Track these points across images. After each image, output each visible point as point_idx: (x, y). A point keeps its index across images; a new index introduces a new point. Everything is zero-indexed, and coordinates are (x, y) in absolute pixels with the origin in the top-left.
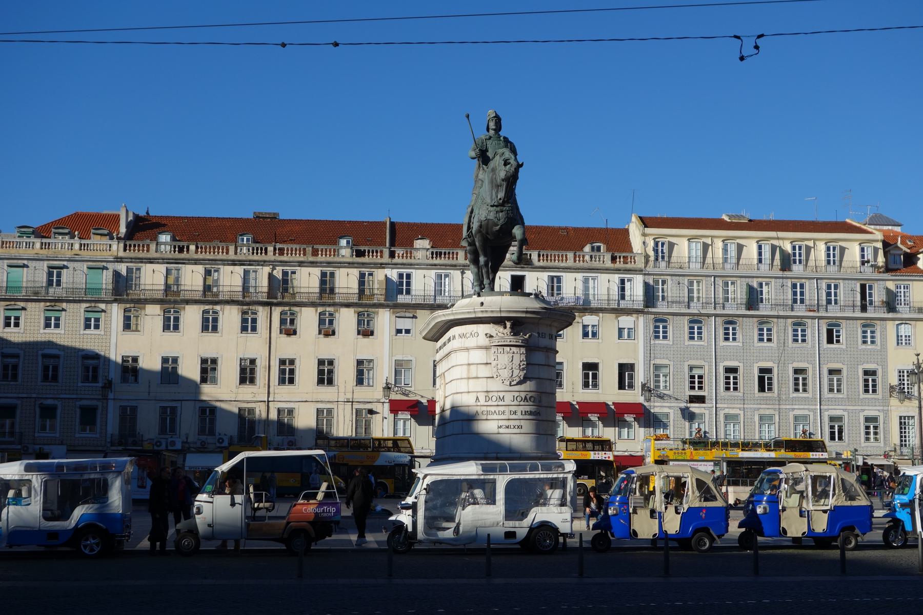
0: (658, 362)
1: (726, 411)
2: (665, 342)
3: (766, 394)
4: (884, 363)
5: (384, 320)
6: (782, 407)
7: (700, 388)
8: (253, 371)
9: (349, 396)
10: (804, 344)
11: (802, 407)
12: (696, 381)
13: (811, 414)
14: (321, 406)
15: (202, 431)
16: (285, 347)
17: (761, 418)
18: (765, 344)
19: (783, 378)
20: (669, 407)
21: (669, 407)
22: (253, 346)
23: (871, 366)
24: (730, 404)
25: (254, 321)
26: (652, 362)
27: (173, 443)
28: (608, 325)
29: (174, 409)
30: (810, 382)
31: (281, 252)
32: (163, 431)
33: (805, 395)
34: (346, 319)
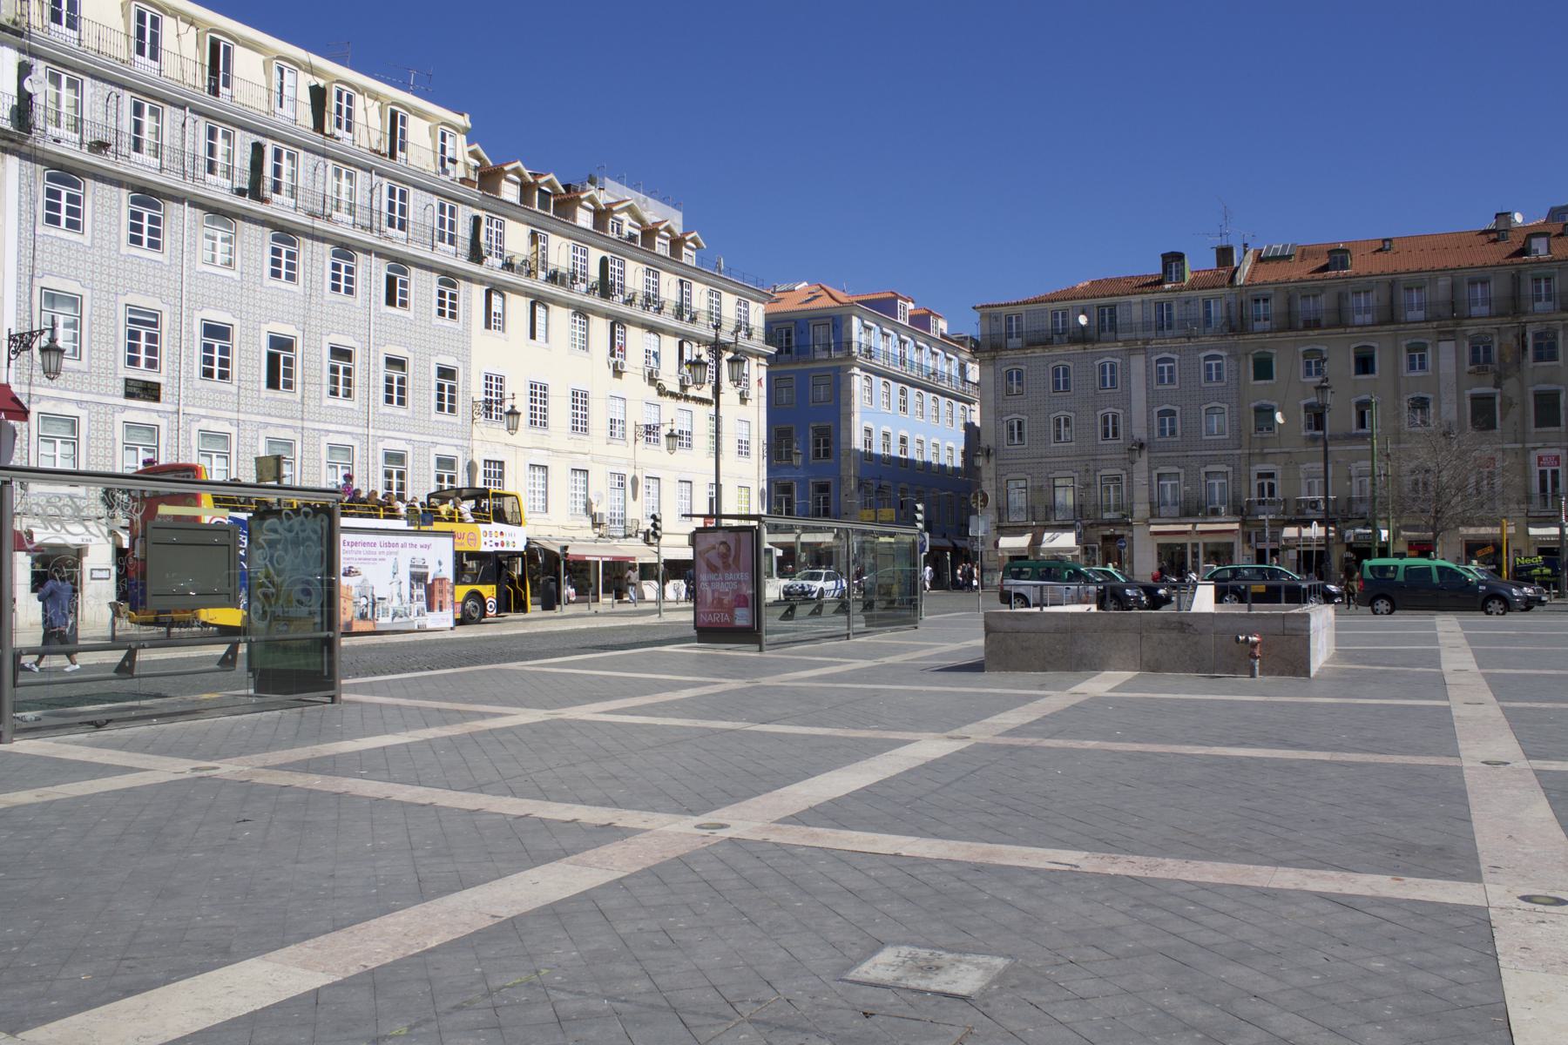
0: (53, 283)
2: (72, 236)
3: (283, 394)
4: (466, 355)
6: (306, 424)
7: (151, 364)
10: (349, 299)
11: (342, 428)
13: (356, 444)
18: (282, 283)
19: (311, 363)
20: (79, 403)
21: (79, 403)
23: (449, 362)
26: (38, 283)
30: (357, 378)
33: (346, 403)
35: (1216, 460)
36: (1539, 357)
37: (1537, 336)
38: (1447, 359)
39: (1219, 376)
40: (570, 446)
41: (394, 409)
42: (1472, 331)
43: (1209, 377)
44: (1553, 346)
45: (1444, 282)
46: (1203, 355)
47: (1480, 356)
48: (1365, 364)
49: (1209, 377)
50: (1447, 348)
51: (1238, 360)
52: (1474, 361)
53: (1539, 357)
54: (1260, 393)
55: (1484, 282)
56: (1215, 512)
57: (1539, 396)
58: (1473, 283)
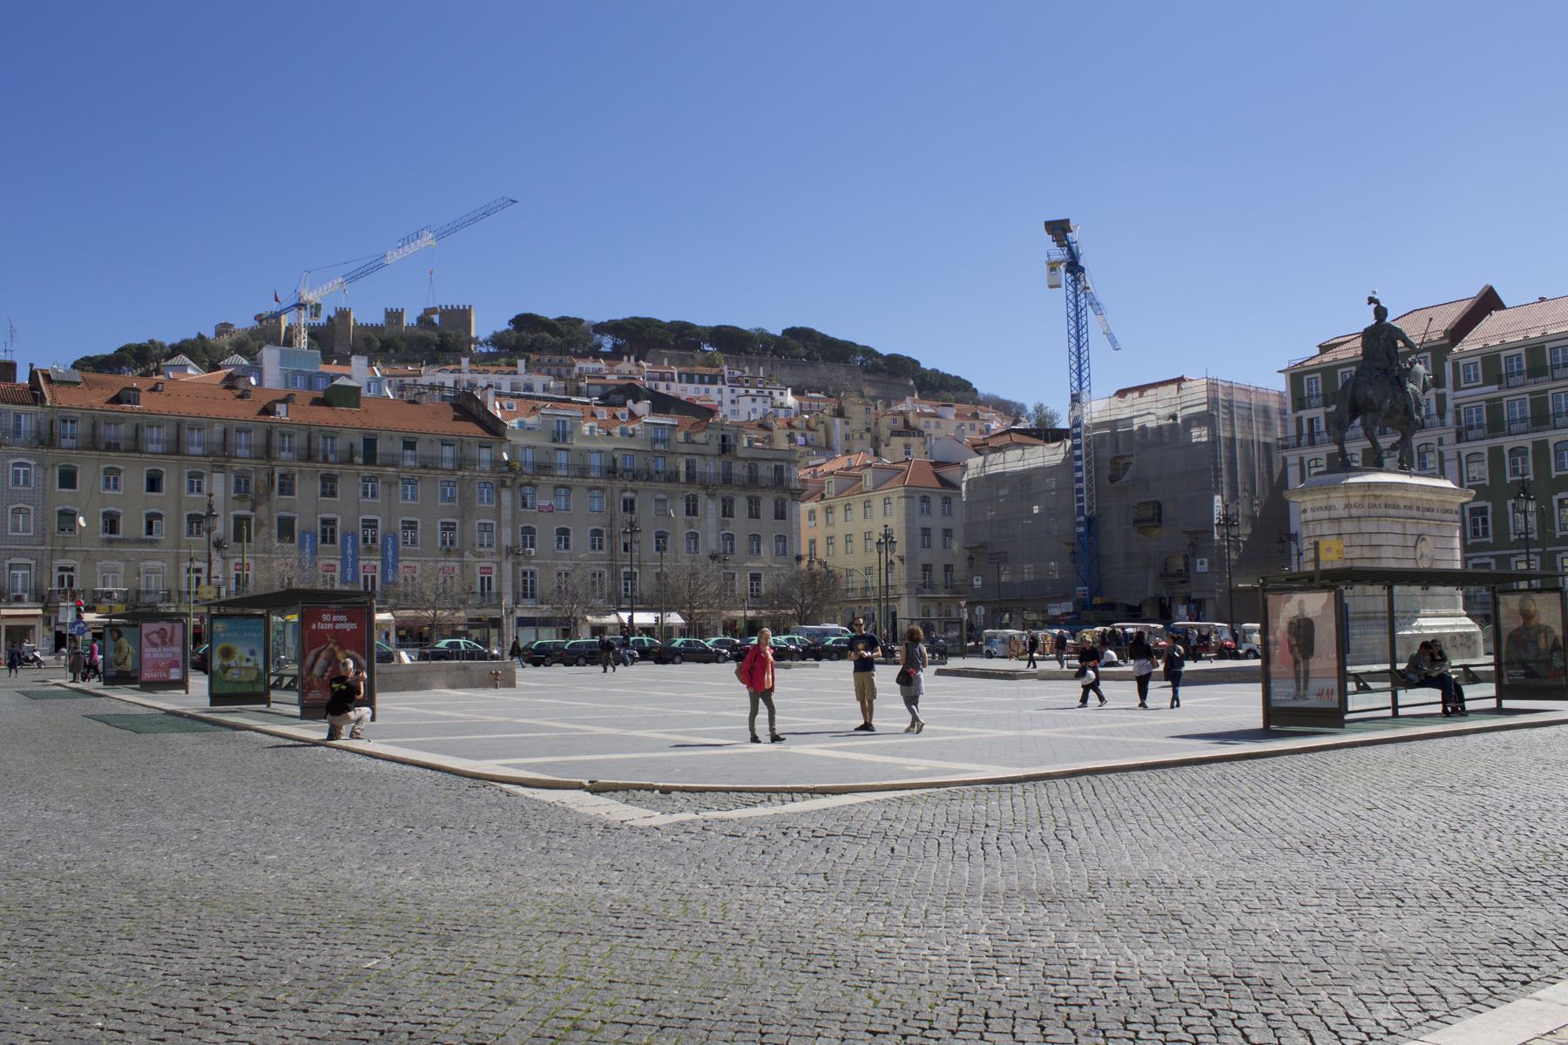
35: (23, 554)
36: (282, 492)
37: (281, 476)
38: (218, 486)
39: (26, 482)
42: (237, 467)
43: (17, 482)
44: (291, 485)
45: (219, 428)
46: (12, 461)
47: (242, 487)
48: (154, 484)
49: (17, 482)
50: (218, 478)
51: (45, 470)
52: (237, 490)
53: (282, 492)
54: (64, 498)
55: (247, 432)
56: (19, 599)
57: (281, 520)
58: (239, 431)
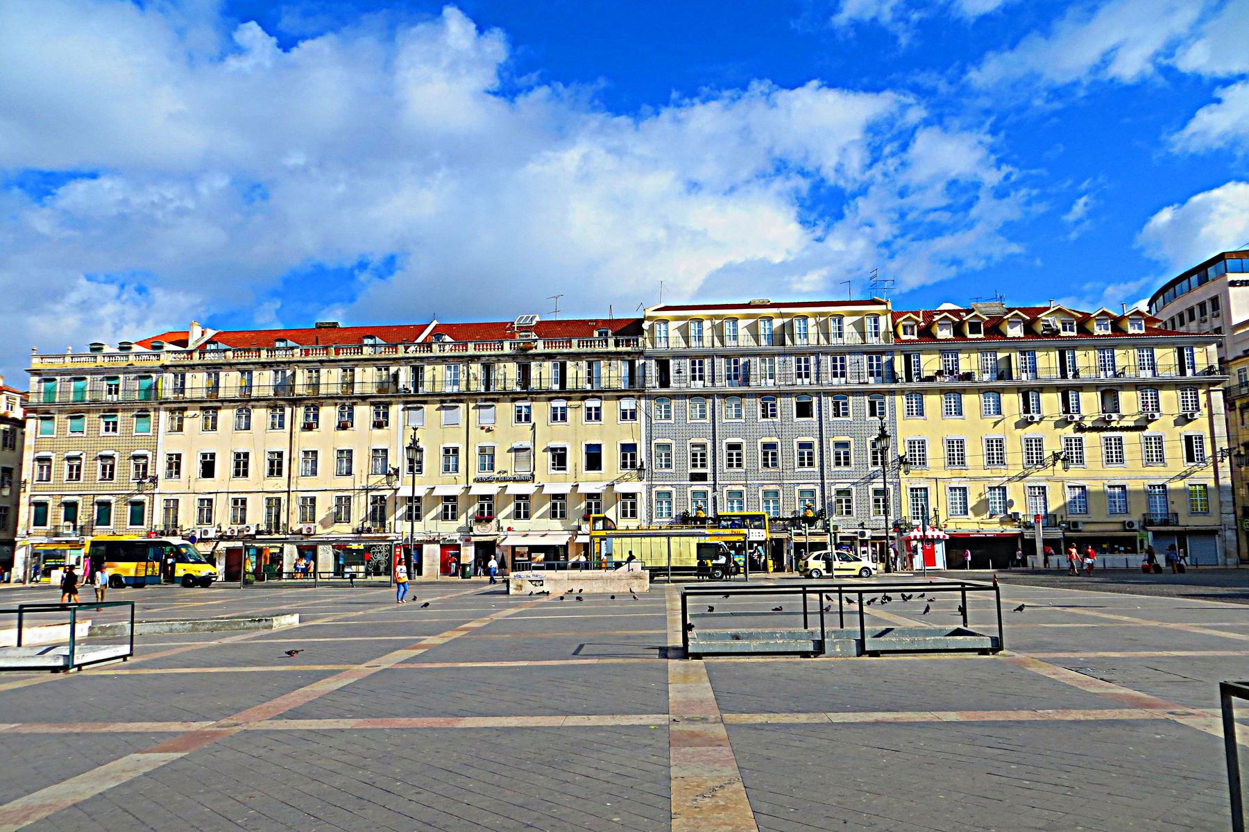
1: (729, 488)
5: (395, 411)
8: (280, 464)
9: (364, 484)
12: (698, 458)
14: (340, 494)
15: (234, 521)
16: (307, 441)
17: (766, 493)
19: (788, 454)
22: (279, 440)
24: (730, 480)
25: (282, 417)
27: (206, 532)
28: (610, 409)
29: (210, 501)
31: (307, 354)
32: (200, 522)
34: (364, 413)
40: (987, 473)
41: (843, 468)
